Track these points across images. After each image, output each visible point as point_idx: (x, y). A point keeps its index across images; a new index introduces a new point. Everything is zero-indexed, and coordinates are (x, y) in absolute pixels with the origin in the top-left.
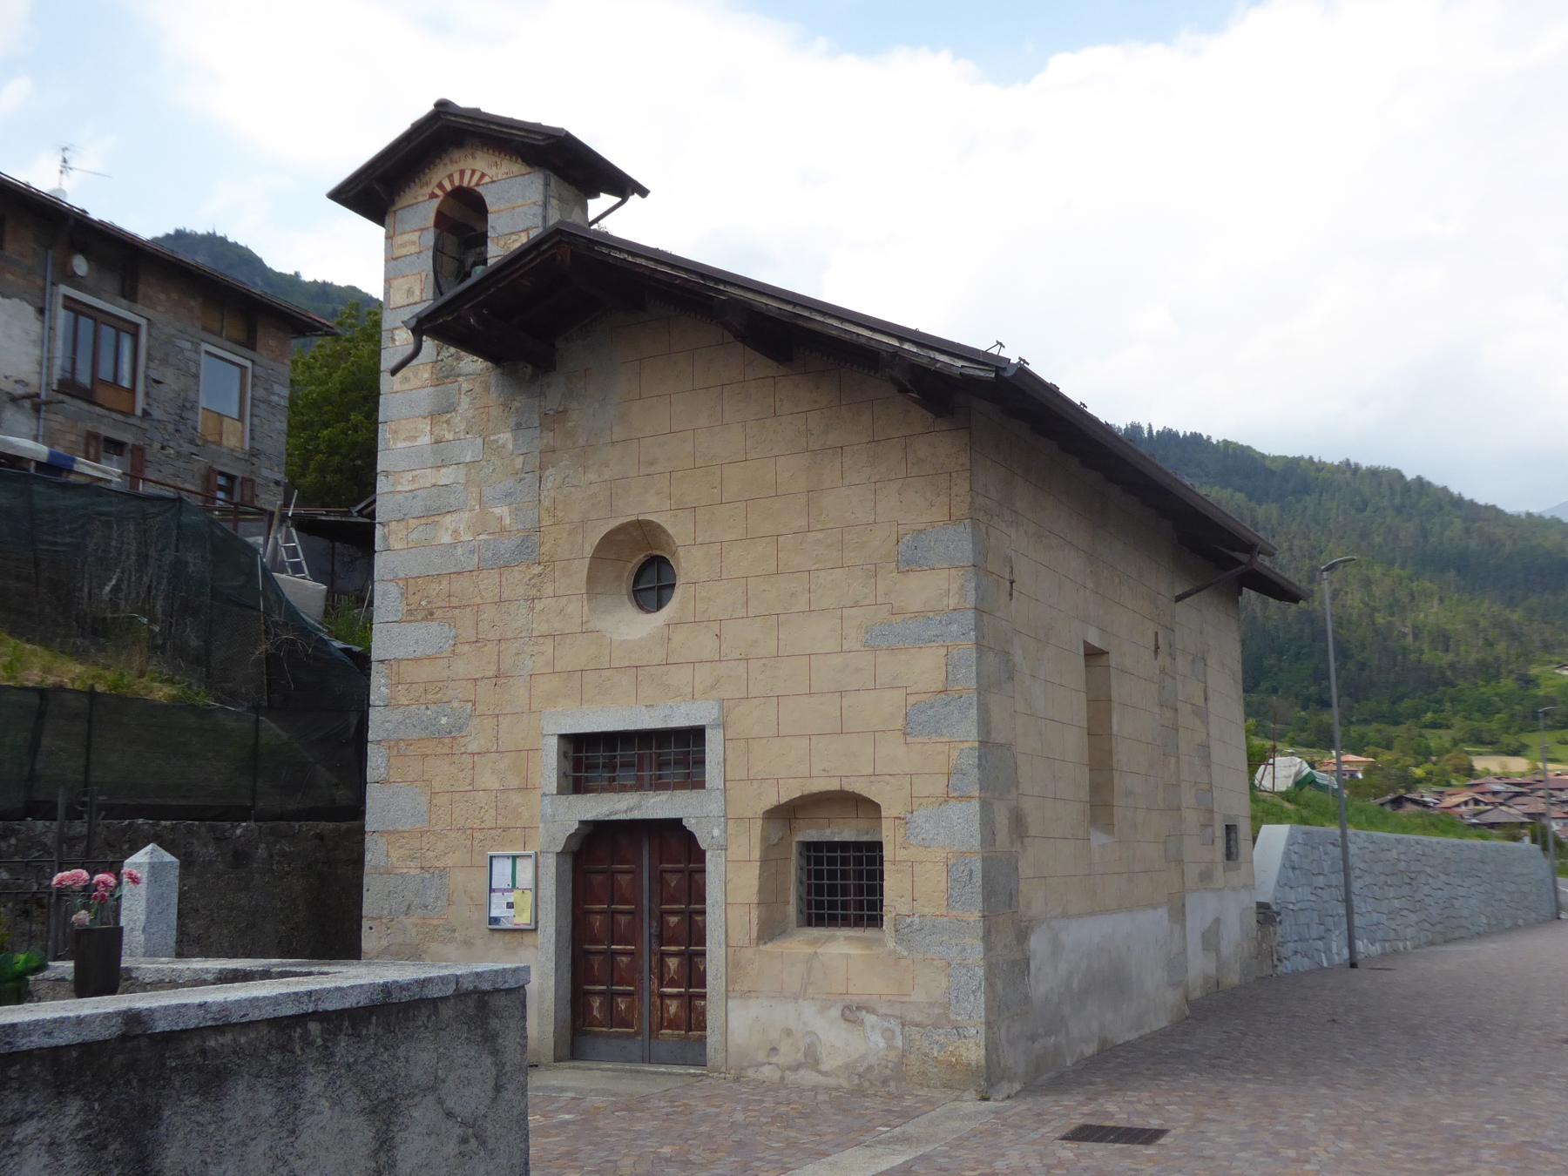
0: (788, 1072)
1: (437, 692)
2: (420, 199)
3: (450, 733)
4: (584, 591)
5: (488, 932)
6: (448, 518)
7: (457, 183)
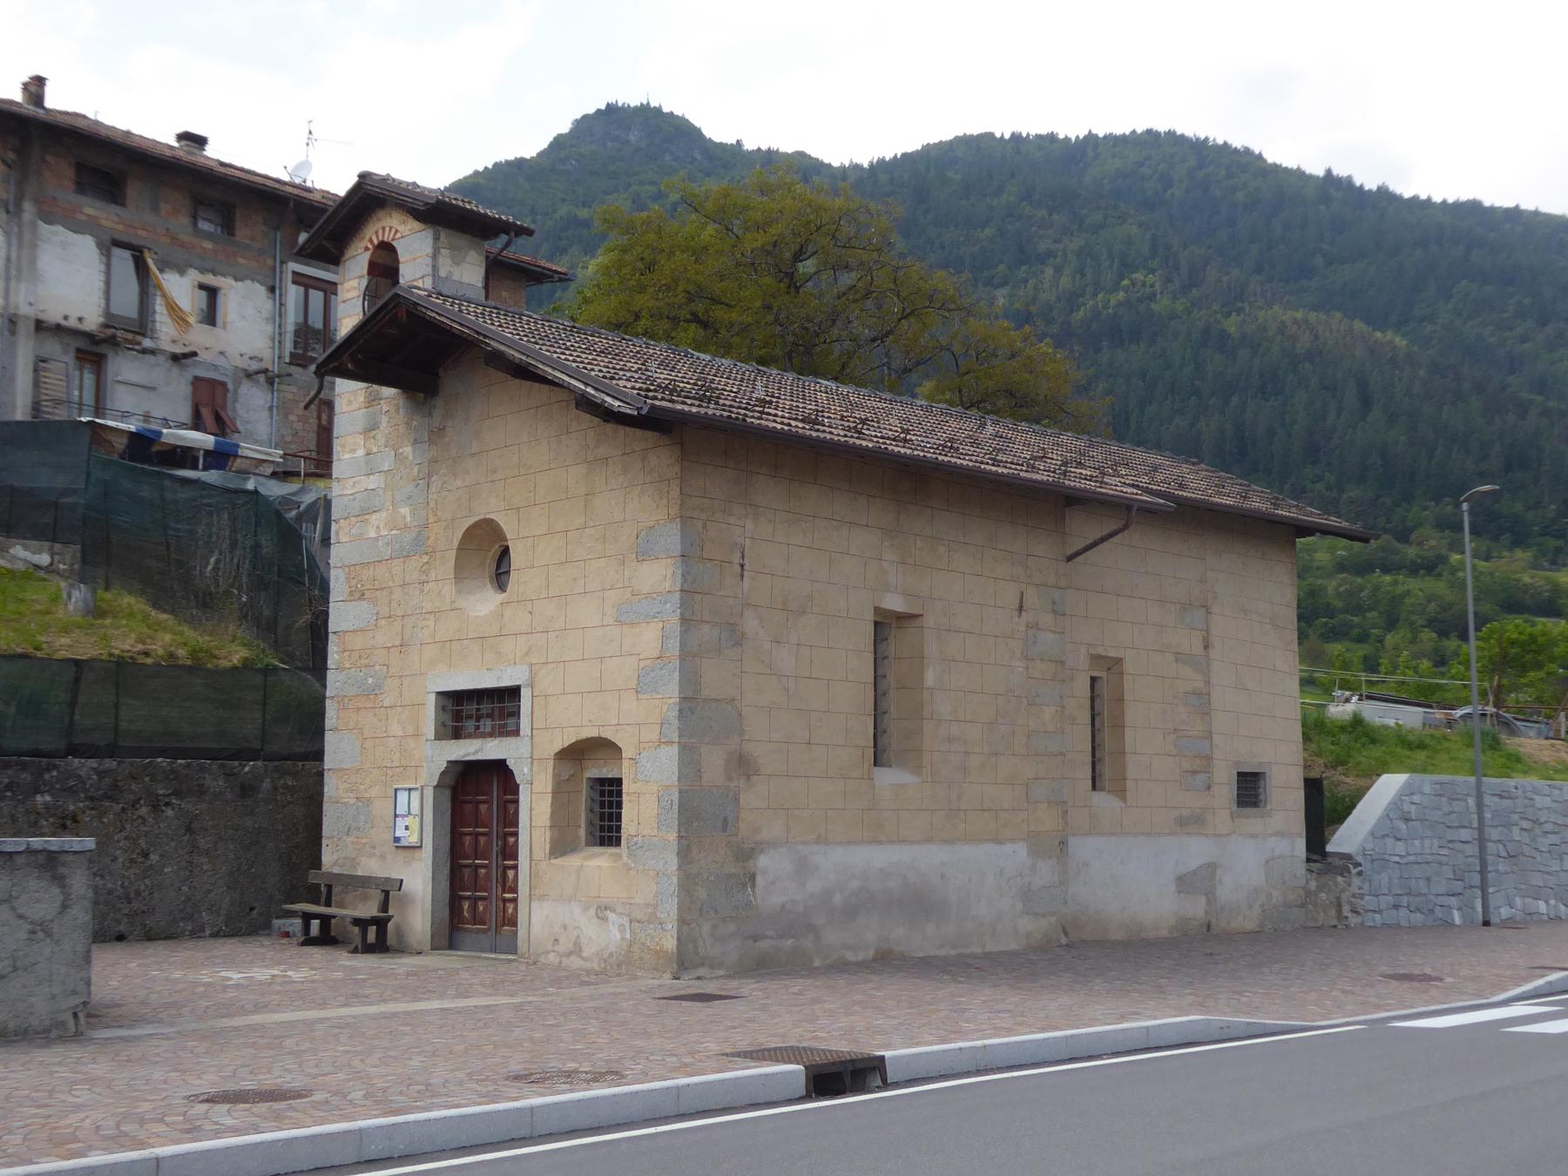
4: (453, 576)
6: (374, 516)
7: (381, 238)
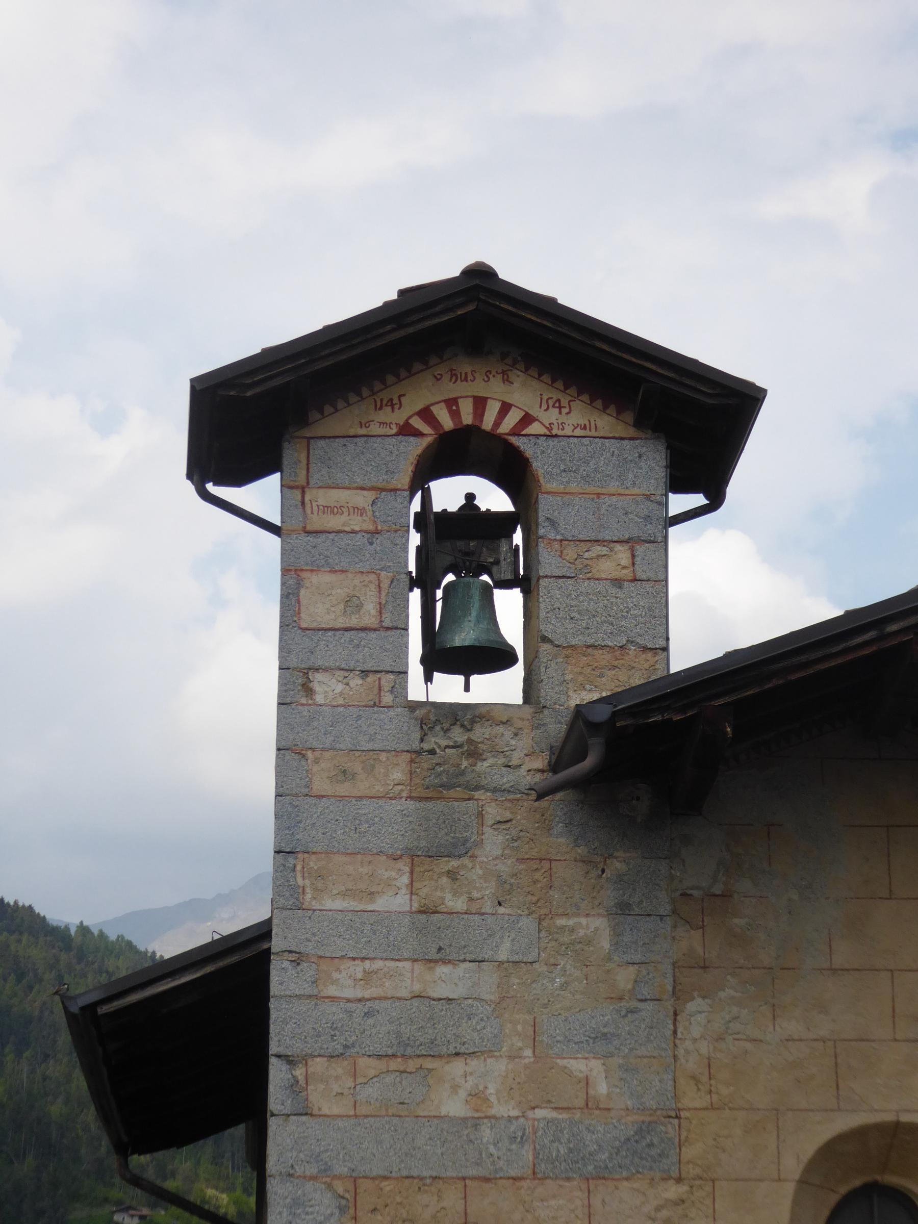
6: (457, 1067)
7: (467, 419)
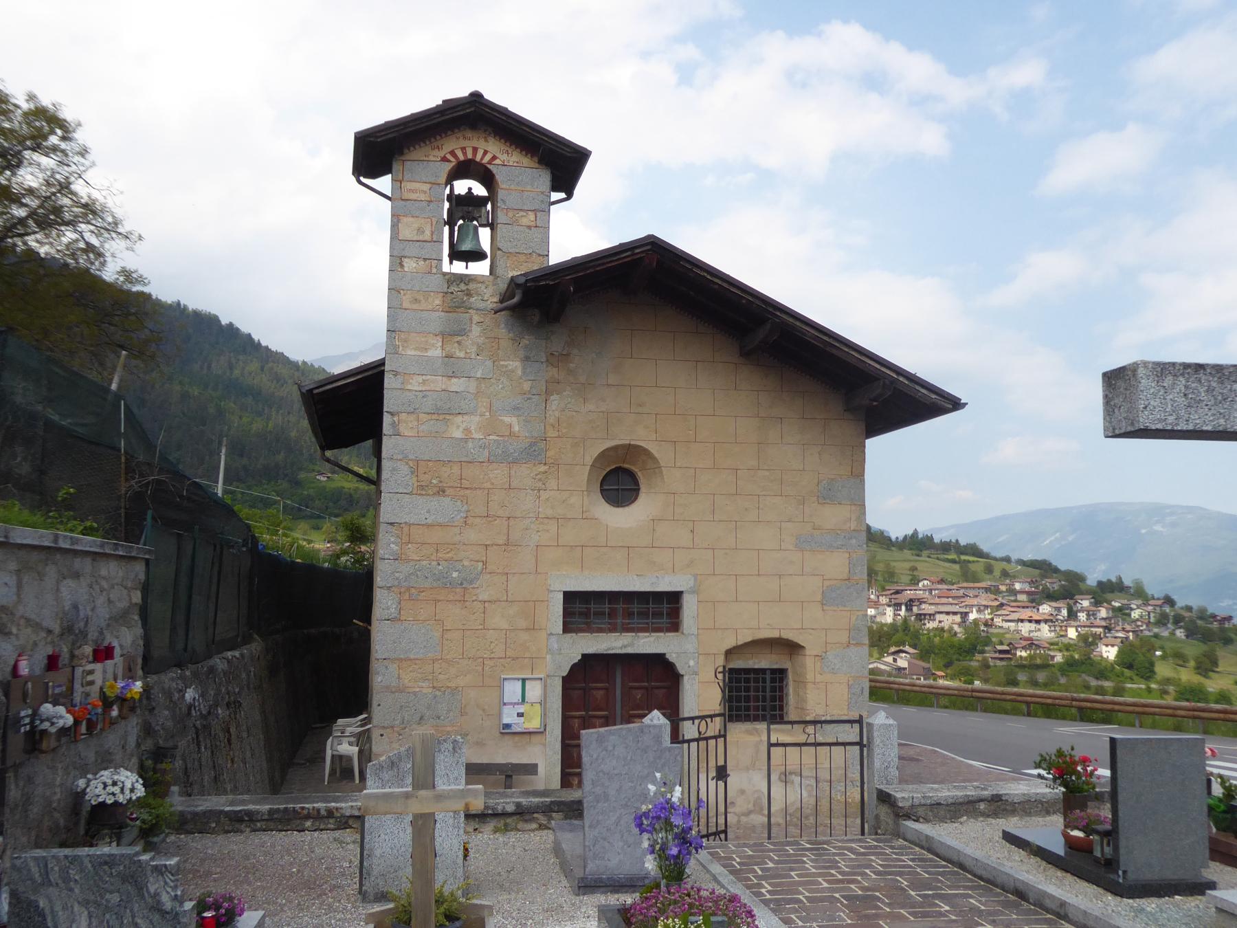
0: (742, 817)
1: (448, 553)
2: (431, 158)
3: (462, 584)
4: (585, 489)
5: (498, 734)
6: (459, 419)
7: (470, 156)
